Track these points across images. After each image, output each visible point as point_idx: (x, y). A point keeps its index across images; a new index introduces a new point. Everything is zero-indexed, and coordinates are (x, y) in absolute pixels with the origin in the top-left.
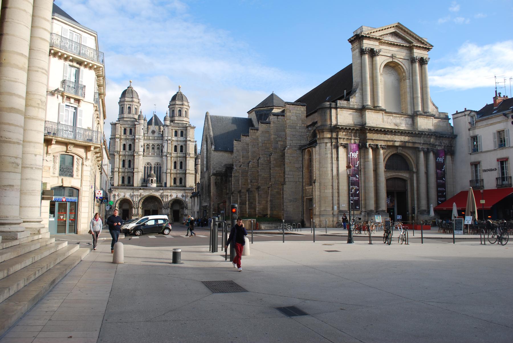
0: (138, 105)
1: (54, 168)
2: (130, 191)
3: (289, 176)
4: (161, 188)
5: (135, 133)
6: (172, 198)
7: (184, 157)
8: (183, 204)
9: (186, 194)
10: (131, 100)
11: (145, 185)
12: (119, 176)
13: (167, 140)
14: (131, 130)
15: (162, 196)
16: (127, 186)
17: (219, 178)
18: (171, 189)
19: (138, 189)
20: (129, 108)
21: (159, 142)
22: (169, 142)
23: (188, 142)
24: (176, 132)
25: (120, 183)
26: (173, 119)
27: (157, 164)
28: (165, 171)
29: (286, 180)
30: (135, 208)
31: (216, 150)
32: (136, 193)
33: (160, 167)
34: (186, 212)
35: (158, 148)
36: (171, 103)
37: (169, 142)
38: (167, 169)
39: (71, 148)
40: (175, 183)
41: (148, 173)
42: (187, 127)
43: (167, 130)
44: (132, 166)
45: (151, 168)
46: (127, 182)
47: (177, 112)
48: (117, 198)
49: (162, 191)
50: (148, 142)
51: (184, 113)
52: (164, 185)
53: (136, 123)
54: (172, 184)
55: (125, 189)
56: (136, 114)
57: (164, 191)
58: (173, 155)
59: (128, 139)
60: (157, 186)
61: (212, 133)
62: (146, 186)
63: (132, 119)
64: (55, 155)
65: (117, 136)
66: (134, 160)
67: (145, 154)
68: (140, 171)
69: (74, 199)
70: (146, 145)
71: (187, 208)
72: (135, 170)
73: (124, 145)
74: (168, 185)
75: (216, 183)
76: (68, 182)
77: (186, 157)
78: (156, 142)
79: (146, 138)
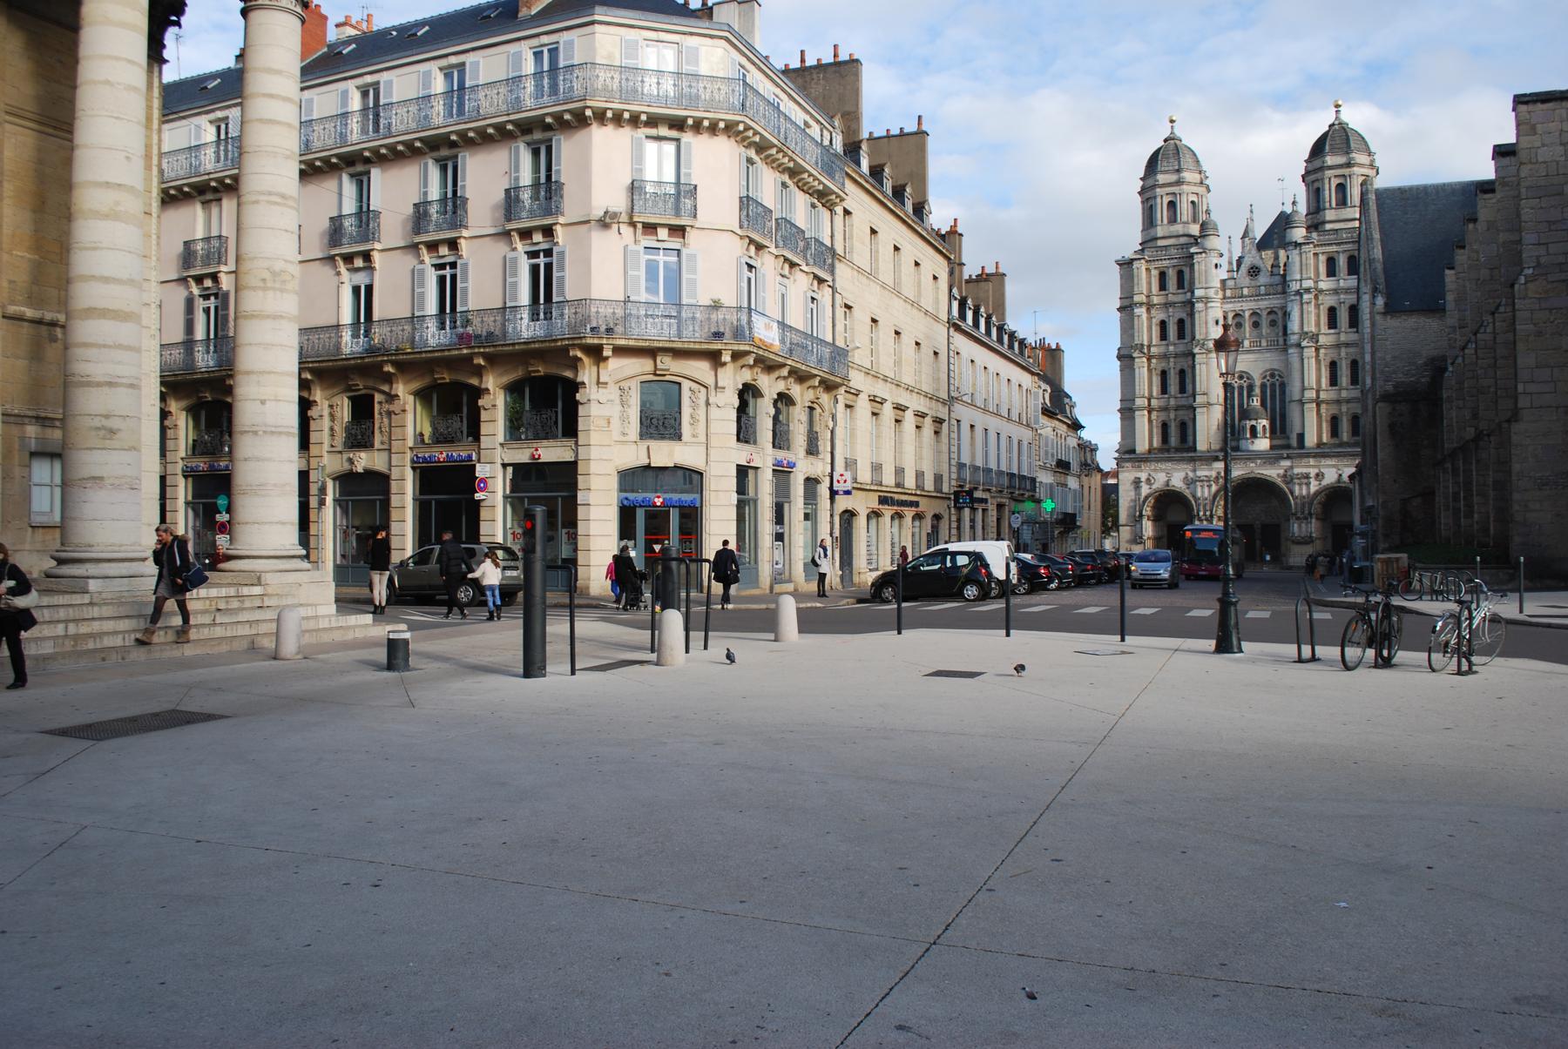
0: (1201, 190)
1: (624, 419)
3: (1532, 388)
4: (1285, 453)
5: (1192, 282)
6: (1325, 483)
10: (1173, 178)
12: (1150, 421)
13: (1298, 293)
14: (1180, 274)
15: (1288, 478)
16: (1177, 450)
18: (1321, 452)
19: (1210, 458)
20: (1172, 204)
21: (1275, 302)
22: (1306, 297)
26: (1319, 218)
27: (1272, 376)
28: (1296, 397)
29: (1523, 402)
31: (1391, 310)
32: (1203, 472)
33: (1283, 385)
35: (1273, 323)
37: (1306, 297)
38: (1303, 389)
39: (666, 362)
40: (1335, 432)
43: (1297, 259)
44: (1189, 388)
45: (1251, 388)
46: (1177, 439)
47: (1330, 195)
48: (1145, 490)
49: (1287, 463)
50: (1237, 307)
52: (1294, 442)
55: (1169, 460)
56: (1195, 220)
57: (1296, 462)
58: (1322, 340)
59: (1172, 304)
60: (1272, 447)
61: (1378, 253)
63: (1183, 240)
64: (622, 384)
65: (1137, 299)
66: (1194, 367)
69: (687, 498)
70: (1230, 316)
72: (1199, 399)
73: (1163, 324)
74: (1311, 440)
75: (1392, 427)
76: (664, 454)
78: (1264, 304)
79: (1228, 293)
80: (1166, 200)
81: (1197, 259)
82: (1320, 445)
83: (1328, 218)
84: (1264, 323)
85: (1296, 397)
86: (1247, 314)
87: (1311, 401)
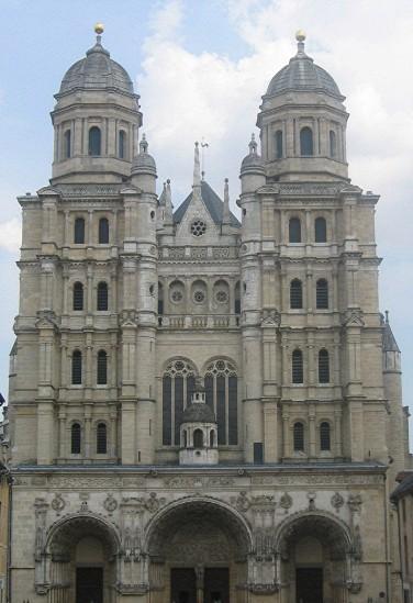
0: (132, 119)
2: (103, 482)
5: (119, 236)
6: (292, 510)
8: (340, 537)
9: (354, 493)
10: (99, 98)
11: (170, 456)
13: (259, 257)
14: (104, 223)
18: (284, 469)
23: (352, 263)
24: (295, 223)
27: (221, 366)
28: (254, 392)
33: (233, 379)
34: (354, 573)
36: (269, 105)
40: (299, 444)
41: (179, 401)
42: (340, 199)
44: (111, 376)
49: (245, 482)
51: (325, 139)
52: (250, 458)
54: (290, 452)
60: (222, 462)
62: (176, 463)
63: (109, 179)
66: (118, 348)
67: (166, 322)
68: (144, 394)
73: (78, 287)
77: (342, 330)
78: (211, 271)
79: (166, 253)
81: (129, 202)
83: (293, 169)
84: (211, 294)
85: (254, 392)
86: (188, 283)
87: (272, 399)
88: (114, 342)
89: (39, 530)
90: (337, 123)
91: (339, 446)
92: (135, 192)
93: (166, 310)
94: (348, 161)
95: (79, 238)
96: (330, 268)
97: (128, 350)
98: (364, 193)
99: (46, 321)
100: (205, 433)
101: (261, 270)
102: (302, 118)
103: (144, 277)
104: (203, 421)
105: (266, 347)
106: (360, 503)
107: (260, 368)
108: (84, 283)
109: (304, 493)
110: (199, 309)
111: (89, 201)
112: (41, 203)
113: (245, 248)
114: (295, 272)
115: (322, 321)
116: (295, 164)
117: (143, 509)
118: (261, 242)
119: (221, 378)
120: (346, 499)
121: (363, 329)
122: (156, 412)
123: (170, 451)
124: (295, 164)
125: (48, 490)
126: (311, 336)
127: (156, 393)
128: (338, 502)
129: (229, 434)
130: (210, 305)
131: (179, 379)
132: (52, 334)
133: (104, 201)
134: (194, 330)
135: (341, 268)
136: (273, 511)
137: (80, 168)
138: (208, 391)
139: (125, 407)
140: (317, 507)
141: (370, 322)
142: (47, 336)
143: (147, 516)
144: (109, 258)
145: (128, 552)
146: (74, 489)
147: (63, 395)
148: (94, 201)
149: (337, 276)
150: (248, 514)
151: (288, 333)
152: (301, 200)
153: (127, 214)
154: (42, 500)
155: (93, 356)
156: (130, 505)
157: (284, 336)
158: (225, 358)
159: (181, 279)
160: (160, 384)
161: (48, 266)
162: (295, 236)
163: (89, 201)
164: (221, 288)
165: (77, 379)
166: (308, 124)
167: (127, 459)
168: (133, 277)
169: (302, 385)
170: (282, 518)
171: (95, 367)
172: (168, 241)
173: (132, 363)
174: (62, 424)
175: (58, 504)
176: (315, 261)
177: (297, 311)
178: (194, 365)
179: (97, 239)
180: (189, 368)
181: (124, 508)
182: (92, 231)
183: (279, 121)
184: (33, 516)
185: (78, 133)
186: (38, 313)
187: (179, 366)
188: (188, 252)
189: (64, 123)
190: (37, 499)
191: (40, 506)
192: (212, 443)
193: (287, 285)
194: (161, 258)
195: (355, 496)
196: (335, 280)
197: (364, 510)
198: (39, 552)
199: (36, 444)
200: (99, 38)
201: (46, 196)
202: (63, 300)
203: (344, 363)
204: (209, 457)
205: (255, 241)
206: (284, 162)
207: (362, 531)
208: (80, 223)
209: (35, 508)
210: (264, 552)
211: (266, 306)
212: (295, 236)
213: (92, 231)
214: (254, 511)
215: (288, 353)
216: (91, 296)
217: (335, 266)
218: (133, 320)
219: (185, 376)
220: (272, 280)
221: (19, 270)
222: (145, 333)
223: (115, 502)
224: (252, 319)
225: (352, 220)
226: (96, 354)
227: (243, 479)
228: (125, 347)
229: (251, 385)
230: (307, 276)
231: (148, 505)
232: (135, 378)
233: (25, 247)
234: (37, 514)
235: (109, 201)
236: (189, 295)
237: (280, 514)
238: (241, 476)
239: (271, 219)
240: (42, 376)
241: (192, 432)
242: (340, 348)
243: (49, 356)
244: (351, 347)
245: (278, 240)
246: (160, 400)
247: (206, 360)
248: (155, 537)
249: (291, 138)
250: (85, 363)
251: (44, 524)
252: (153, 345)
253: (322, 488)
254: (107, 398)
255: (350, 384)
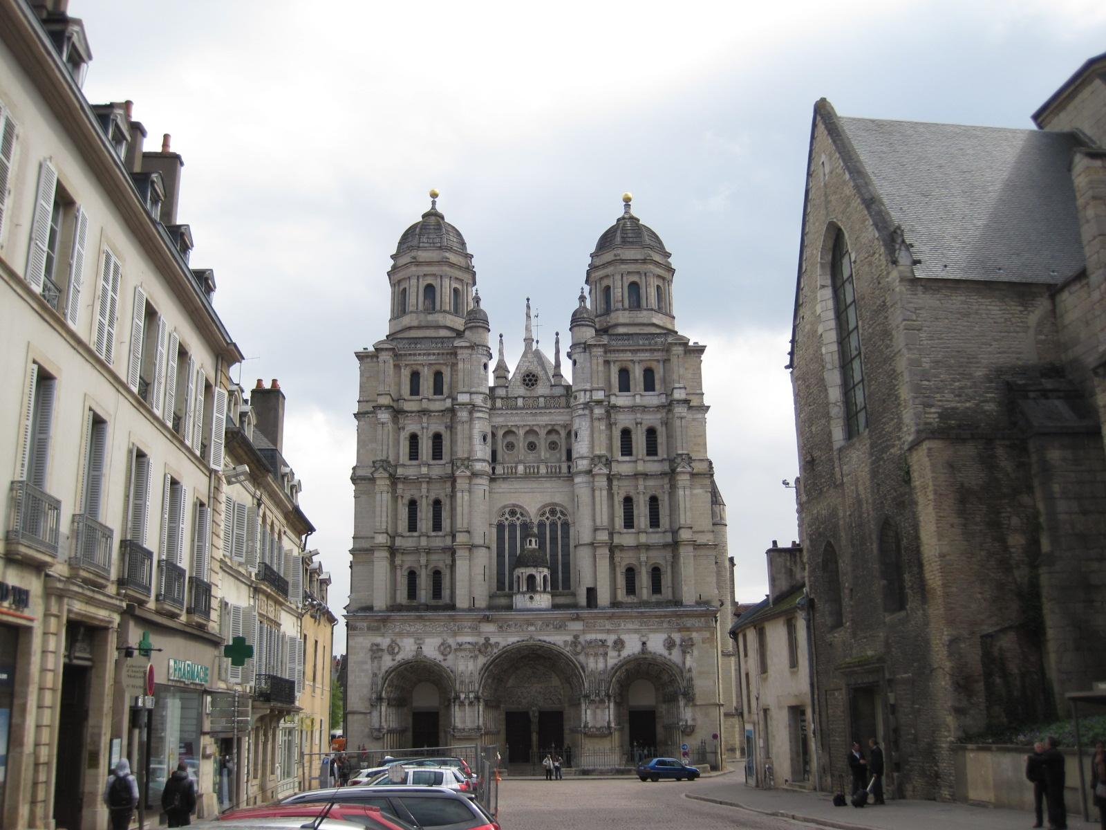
0: (466, 277)
6: (625, 653)
7: (663, 474)
8: (672, 681)
9: (686, 634)
11: (503, 601)
14: (438, 376)
16: (428, 608)
17: (969, 450)
21: (558, 417)
23: (680, 410)
24: (624, 374)
25: (402, 597)
27: (553, 512)
28: (586, 537)
30: (462, 704)
33: (566, 525)
35: (553, 446)
36: (598, 262)
40: (631, 589)
42: (667, 349)
44: (446, 523)
51: (653, 292)
52: (583, 600)
53: (457, 343)
54: (621, 595)
56: (456, 312)
60: (555, 607)
62: (510, 608)
66: (453, 496)
67: (499, 470)
68: (478, 540)
70: (500, 433)
71: (689, 697)
72: (461, 538)
73: (414, 439)
77: (672, 474)
78: (544, 420)
79: (499, 403)
80: (423, 283)
81: (463, 354)
82: (615, 604)
83: (621, 320)
86: (521, 432)
87: (603, 544)
88: (449, 490)
89: (375, 675)
90: (664, 279)
91: (670, 589)
92: (468, 344)
93: (499, 457)
94: (675, 313)
95: (415, 390)
96: (659, 416)
97: (462, 498)
98: (691, 343)
99: (381, 470)
100: (538, 578)
101: (592, 418)
102: (629, 273)
103: (477, 426)
104: (535, 566)
105: (597, 493)
106: (692, 645)
107: (591, 513)
108: (419, 433)
109: (636, 637)
110: (531, 457)
111: (424, 354)
112: (378, 357)
113: (576, 398)
114: (624, 420)
115: (653, 467)
116: (622, 317)
117: (477, 653)
118: (591, 391)
119: (553, 524)
120: (678, 641)
121: (693, 475)
122: (490, 558)
123: (505, 596)
124: (622, 317)
125: (383, 635)
126: (641, 482)
127: (490, 540)
128: (670, 645)
129: (561, 581)
130: (543, 454)
131: (512, 526)
132: (388, 482)
133: (438, 354)
134: (527, 476)
135: (670, 416)
136: (606, 654)
137: (415, 323)
138: (541, 537)
139: (459, 553)
140: (649, 649)
141: (699, 467)
142: (383, 483)
143: (482, 660)
144: (443, 408)
145: (463, 696)
146: (409, 634)
147: (399, 542)
148: (429, 354)
149: (666, 424)
150: (582, 658)
151: (619, 479)
152: (630, 351)
153: (460, 366)
154: (377, 645)
155: (428, 505)
156: (465, 650)
157: (615, 483)
158: (556, 504)
159: (514, 429)
160: (494, 530)
161: (384, 416)
162: (625, 386)
163: (424, 354)
164: (554, 437)
165: (412, 527)
166: (635, 278)
167: (462, 602)
168: (466, 426)
169: (633, 530)
170: (615, 661)
171: (431, 515)
172: (501, 392)
173: (466, 511)
174: (399, 572)
175: (393, 649)
176: (644, 409)
177: (627, 458)
178: (527, 512)
179: (432, 391)
180: (522, 514)
181: (459, 652)
182: (427, 384)
183: (607, 276)
184: (369, 661)
185: (413, 290)
186: (374, 462)
187: (513, 513)
188: (520, 402)
189: (399, 282)
190: (373, 645)
191: (376, 651)
192: (545, 588)
193: (617, 434)
194: (493, 408)
195: (686, 638)
196: (664, 426)
197: (696, 653)
198: (374, 696)
199: (373, 591)
200: (434, 203)
201: (382, 349)
202: (399, 450)
203: (673, 508)
204: (543, 600)
205: (585, 391)
206: (613, 315)
207: (694, 674)
208: (415, 376)
209: (371, 653)
210: (598, 695)
211: (597, 452)
212: (625, 386)
213: (427, 384)
214: (587, 655)
215: (619, 500)
216: (425, 447)
217: (664, 414)
218: (467, 467)
219: (518, 523)
220: (603, 427)
221: (356, 422)
222: (478, 481)
223: (450, 646)
224: (583, 465)
225: (679, 367)
226: (431, 502)
227: (576, 622)
228: (459, 495)
229: (583, 531)
230: (637, 424)
231: (483, 649)
232: (470, 523)
233: (362, 399)
234: (373, 659)
235: (443, 354)
236: (521, 444)
237: (611, 658)
238: (573, 620)
239: (601, 368)
240: (378, 524)
241: (525, 577)
242: (670, 493)
243: (384, 503)
244: (681, 492)
245: (608, 390)
246: (494, 546)
247: (539, 506)
248: (490, 681)
249: (619, 292)
250: (420, 511)
251: (380, 669)
252: (487, 493)
253: (655, 631)
254: (442, 545)
255: (680, 528)
